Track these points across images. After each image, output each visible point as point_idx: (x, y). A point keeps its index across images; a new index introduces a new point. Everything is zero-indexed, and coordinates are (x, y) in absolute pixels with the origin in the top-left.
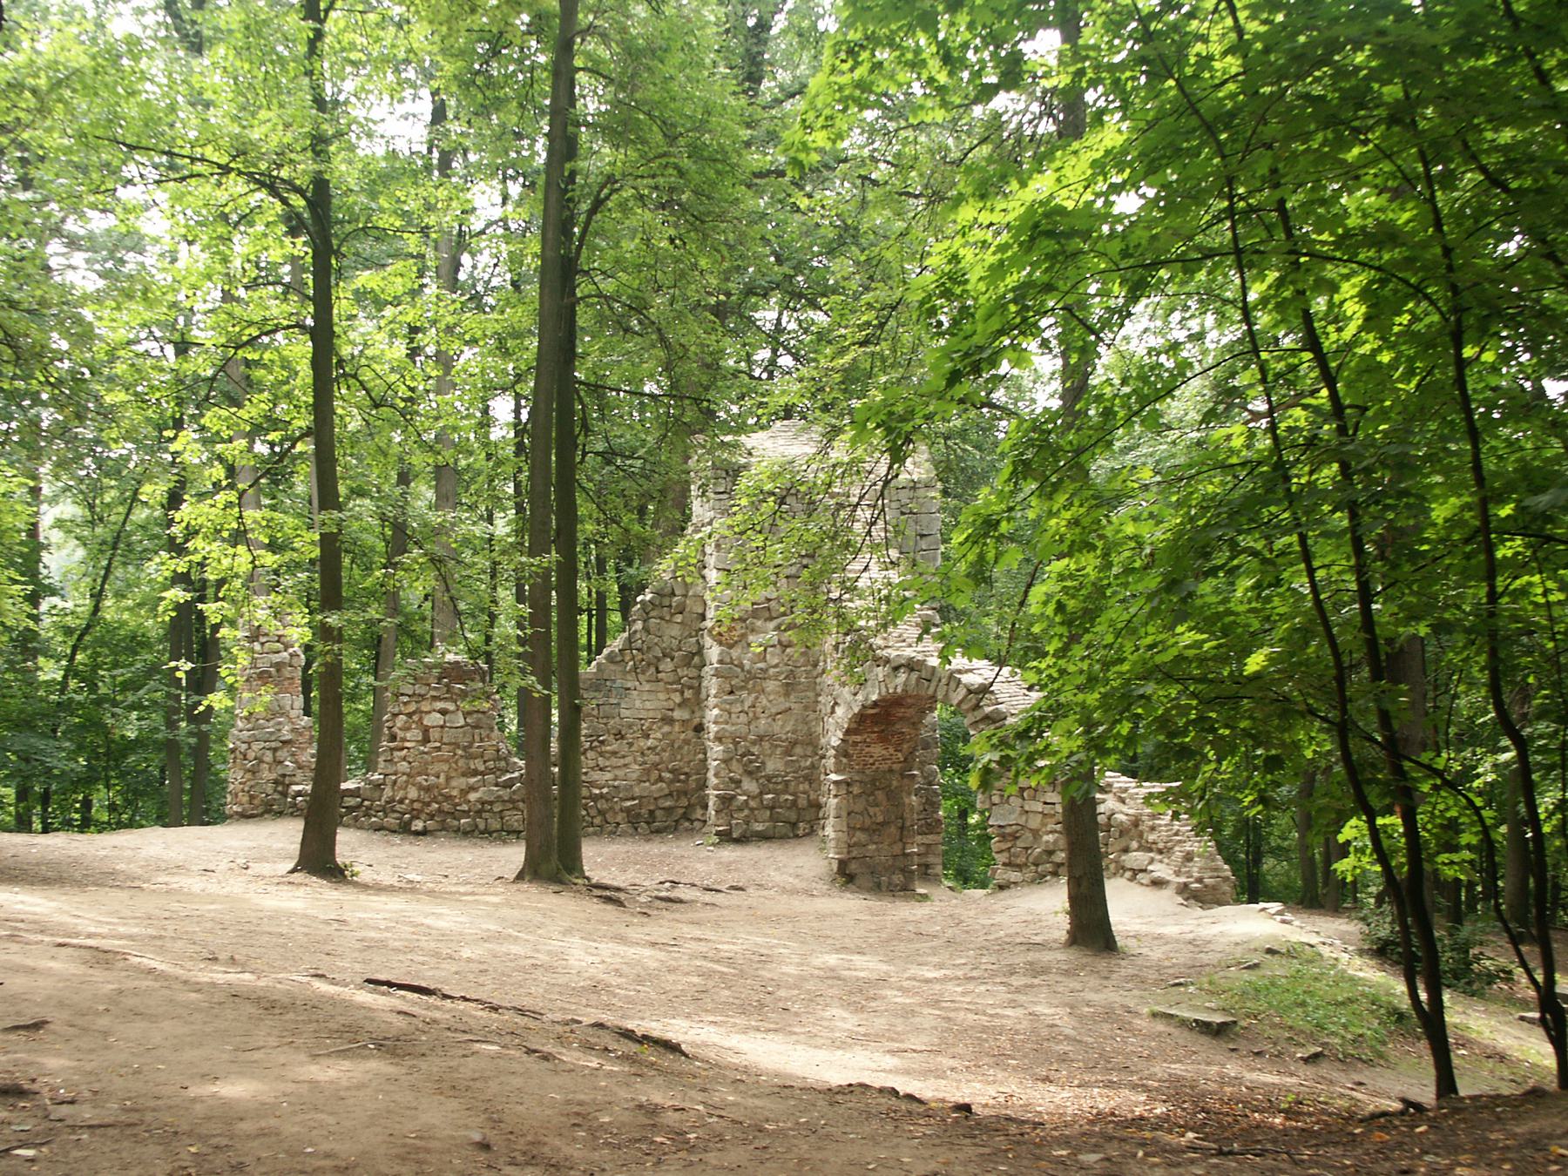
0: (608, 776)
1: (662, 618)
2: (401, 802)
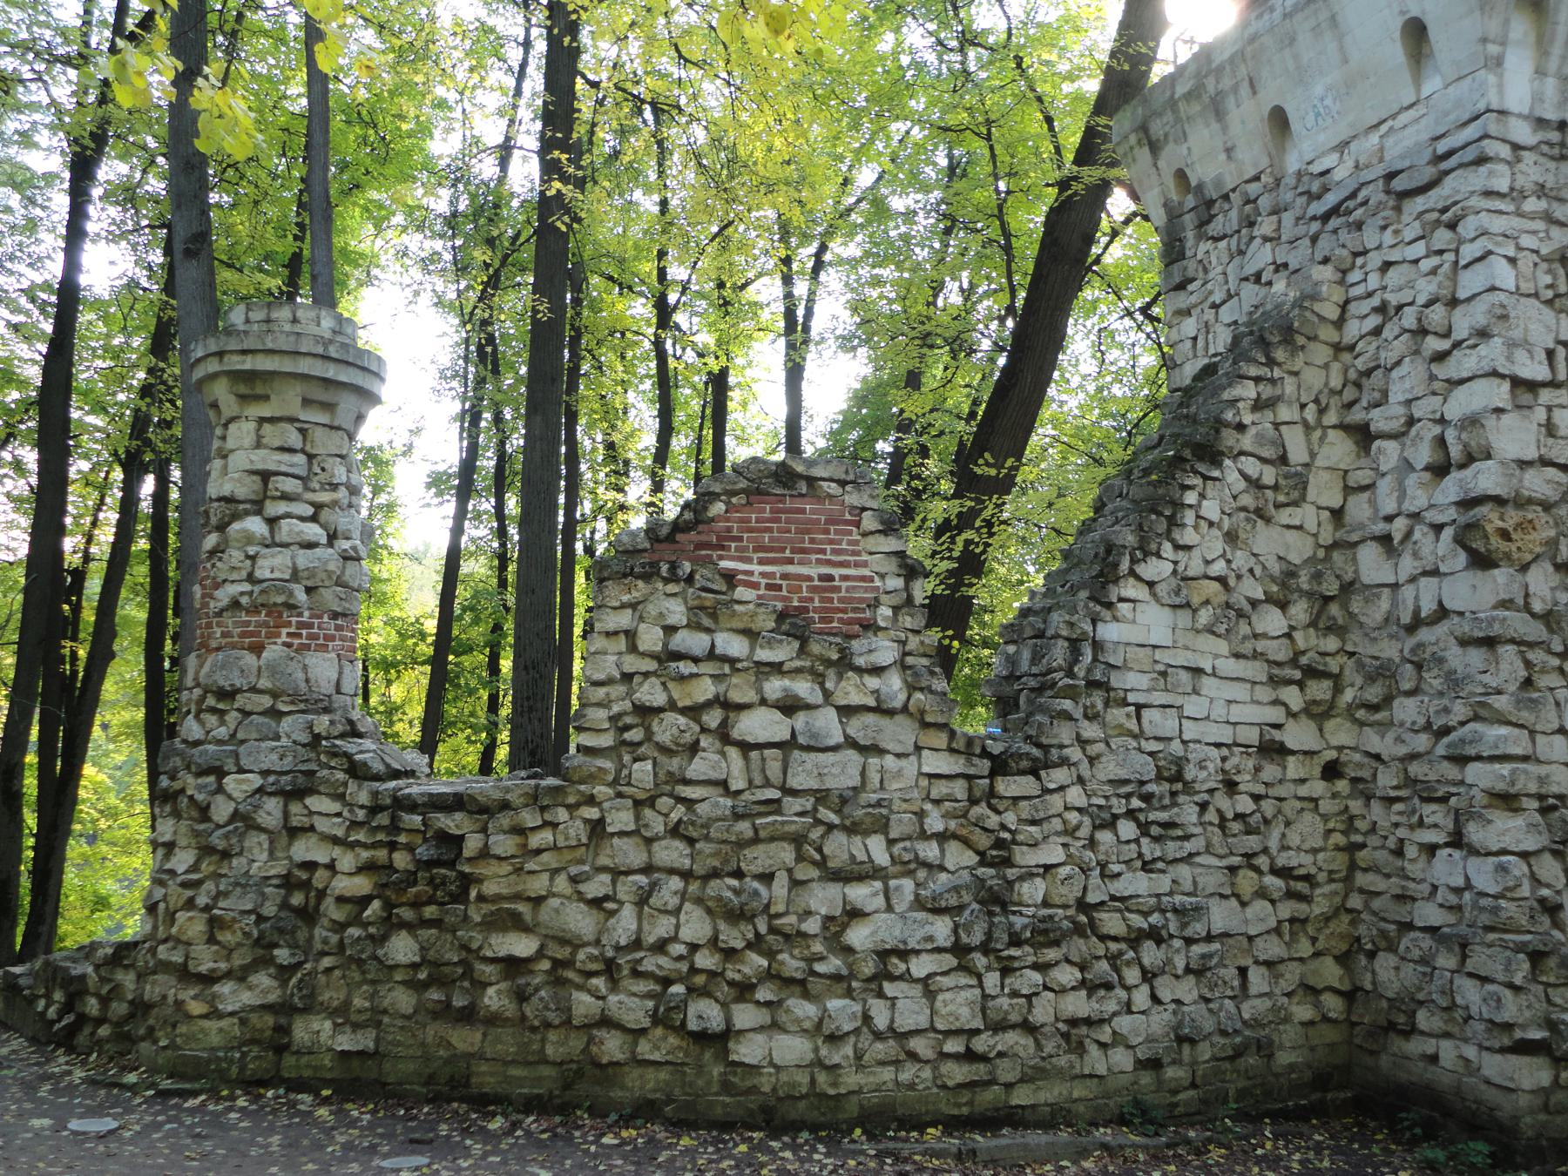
0: (1164, 883)
1: (1259, 513)
2: (661, 947)
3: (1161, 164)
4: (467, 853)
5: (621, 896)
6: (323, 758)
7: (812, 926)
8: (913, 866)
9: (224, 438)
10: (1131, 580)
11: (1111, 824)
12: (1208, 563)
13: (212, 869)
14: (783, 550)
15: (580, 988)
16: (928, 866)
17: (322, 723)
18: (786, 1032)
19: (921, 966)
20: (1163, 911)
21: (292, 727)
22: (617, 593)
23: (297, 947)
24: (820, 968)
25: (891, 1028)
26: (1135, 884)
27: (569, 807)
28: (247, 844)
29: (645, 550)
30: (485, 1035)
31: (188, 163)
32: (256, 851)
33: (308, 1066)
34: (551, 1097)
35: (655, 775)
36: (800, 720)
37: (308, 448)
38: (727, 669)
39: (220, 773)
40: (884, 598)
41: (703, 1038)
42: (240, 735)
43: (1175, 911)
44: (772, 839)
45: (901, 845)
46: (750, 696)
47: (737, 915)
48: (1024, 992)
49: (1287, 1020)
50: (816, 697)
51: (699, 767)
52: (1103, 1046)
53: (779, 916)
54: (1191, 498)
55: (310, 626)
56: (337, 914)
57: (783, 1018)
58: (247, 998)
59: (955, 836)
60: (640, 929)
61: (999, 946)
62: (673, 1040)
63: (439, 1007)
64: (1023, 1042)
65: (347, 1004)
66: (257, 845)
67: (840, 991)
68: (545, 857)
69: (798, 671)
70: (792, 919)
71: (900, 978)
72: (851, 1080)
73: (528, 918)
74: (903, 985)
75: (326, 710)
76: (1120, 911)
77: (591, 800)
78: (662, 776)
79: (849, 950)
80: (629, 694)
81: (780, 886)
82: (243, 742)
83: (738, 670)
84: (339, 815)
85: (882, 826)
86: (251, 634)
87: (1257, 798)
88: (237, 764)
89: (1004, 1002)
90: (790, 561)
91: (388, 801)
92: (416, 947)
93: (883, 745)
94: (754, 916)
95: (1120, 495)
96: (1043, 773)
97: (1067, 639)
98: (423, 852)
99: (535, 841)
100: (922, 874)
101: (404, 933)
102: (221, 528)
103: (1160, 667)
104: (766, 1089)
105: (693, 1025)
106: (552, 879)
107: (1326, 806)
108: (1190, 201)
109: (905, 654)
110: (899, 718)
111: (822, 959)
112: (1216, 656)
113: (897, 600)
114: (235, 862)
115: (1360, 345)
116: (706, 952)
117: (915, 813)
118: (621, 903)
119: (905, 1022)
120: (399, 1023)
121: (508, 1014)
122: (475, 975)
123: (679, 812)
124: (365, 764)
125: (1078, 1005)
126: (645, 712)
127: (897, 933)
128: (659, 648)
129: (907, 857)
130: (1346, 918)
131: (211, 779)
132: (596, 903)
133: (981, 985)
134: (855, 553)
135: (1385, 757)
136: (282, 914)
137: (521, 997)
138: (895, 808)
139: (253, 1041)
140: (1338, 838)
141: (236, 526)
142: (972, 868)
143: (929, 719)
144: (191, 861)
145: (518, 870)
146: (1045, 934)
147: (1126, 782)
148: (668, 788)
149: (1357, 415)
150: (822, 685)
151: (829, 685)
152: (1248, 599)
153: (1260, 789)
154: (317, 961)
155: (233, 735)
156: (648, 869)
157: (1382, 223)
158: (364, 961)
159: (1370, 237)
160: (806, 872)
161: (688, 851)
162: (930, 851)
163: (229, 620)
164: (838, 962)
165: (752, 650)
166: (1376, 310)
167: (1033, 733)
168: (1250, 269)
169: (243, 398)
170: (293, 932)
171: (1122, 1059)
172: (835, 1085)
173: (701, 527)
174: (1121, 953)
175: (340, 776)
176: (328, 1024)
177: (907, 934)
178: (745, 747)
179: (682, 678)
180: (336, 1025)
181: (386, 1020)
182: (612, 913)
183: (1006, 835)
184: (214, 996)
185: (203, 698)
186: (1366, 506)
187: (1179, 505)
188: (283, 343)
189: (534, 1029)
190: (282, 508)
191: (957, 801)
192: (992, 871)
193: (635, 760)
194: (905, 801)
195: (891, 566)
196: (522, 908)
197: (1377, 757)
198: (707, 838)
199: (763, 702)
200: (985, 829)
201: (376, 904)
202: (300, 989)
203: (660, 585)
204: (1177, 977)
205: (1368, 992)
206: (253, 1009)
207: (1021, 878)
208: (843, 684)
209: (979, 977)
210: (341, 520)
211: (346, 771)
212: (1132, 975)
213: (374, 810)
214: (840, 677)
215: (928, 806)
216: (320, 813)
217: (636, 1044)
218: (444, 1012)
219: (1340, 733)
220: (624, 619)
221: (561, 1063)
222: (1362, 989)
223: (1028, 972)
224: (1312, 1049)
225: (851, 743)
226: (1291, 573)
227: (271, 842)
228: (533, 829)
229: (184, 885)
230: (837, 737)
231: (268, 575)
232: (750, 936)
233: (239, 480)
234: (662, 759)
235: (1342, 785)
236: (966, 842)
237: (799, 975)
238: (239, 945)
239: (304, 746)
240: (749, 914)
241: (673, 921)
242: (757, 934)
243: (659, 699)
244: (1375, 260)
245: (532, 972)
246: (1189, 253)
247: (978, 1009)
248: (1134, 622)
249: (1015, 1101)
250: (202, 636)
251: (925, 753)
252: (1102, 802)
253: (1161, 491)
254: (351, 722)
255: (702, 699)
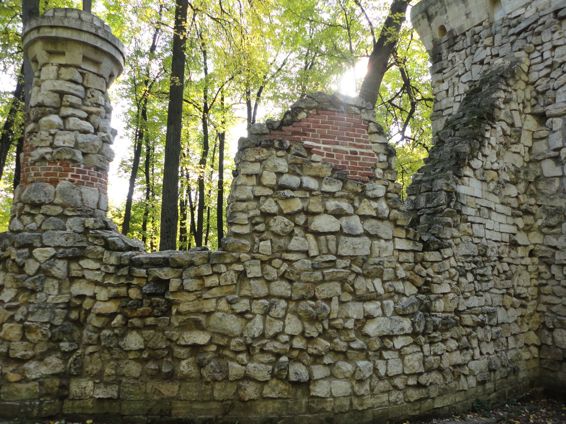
2: (275, 337)
3: (432, 25)
4: (171, 289)
5: (255, 311)
6: (90, 240)
7: (350, 324)
8: (393, 294)
9: (39, 77)
10: (468, 168)
11: (464, 275)
12: (492, 163)
13: (25, 299)
14: (334, 138)
15: (232, 360)
16: (398, 293)
17: (90, 222)
18: (337, 378)
19: (399, 343)
20: (483, 313)
21: (73, 224)
22: (252, 155)
23: (74, 341)
24: (354, 345)
25: (386, 375)
26: (474, 302)
27: (226, 264)
28: (46, 285)
29: (266, 134)
30: (180, 387)
31: (30, 12)
32: (51, 289)
33: (79, 407)
34: (217, 419)
35: (272, 247)
36: (344, 221)
37: (85, 83)
38: (308, 195)
39: (31, 247)
40: (379, 165)
41: (297, 384)
42: (43, 227)
43: (488, 313)
44: (331, 281)
45: (388, 283)
46: (320, 209)
47: (314, 320)
48: (439, 353)
49: (520, 359)
50: (350, 210)
51: (294, 244)
52: (465, 376)
53: (334, 319)
54: (487, 135)
55: (84, 172)
56: (97, 323)
57: (336, 372)
58: (44, 370)
59: (408, 280)
60: (264, 328)
61: (430, 332)
62: (282, 386)
63: (155, 372)
64: (438, 377)
65: (102, 371)
66: (51, 287)
67: (362, 357)
68: (214, 291)
69: (342, 197)
70: (340, 321)
71: (390, 349)
72: (369, 402)
73: (204, 323)
74: (391, 353)
75: (91, 216)
76: (469, 314)
77: (239, 261)
78: (276, 248)
79: (367, 336)
80: (258, 207)
81: (335, 304)
82: (45, 231)
83: (314, 195)
84: (99, 269)
85: (380, 275)
86: (51, 174)
87: (509, 264)
88: (41, 242)
89: (431, 358)
90: (337, 144)
91: (127, 262)
92: (142, 340)
93: (380, 235)
94: (323, 320)
95: (451, 136)
96: (442, 250)
97: (446, 191)
98: (147, 289)
99: (209, 282)
100: (396, 297)
101: (135, 333)
102: (36, 121)
103: (478, 207)
104: (329, 409)
105: (293, 378)
106: (217, 302)
107: (531, 268)
108: (445, 38)
109: (387, 192)
110: (386, 222)
111: (354, 341)
112: (496, 203)
113: (385, 166)
114: (38, 295)
115: (537, 83)
116: (299, 339)
117: (393, 268)
118: (255, 314)
119: (392, 372)
120: (132, 381)
121: (193, 375)
122: (175, 354)
123: (284, 267)
124: (114, 242)
125: (457, 358)
126: (266, 215)
127: (389, 327)
128: (274, 183)
129: (391, 289)
130: (537, 315)
131: (26, 250)
132: (241, 315)
133: (422, 351)
134: (366, 142)
135: (560, 247)
136: (65, 324)
137: (200, 365)
138: (385, 265)
139: (47, 394)
140: (535, 282)
141: (44, 119)
142: (416, 295)
143: (399, 223)
144: (13, 296)
145: (199, 298)
146: (446, 326)
147: (468, 256)
148: (278, 255)
149: (539, 109)
150: (352, 204)
151: (356, 204)
152: (504, 180)
153: (510, 261)
154: (85, 348)
155: (39, 227)
156: (268, 297)
157: (553, 30)
158: (112, 348)
159: (545, 37)
160: (347, 297)
161: (289, 287)
162: (399, 286)
163: (39, 167)
164: (362, 342)
165: (320, 186)
166: (547, 67)
167: (436, 232)
168: (477, 59)
169: (50, 53)
170: (71, 333)
171: (472, 381)
172: (362, 405)
173: (295, 124)
174: (471, 333)
175: (100, 249)
176: (91, 383)
177: (393, 327)
178: (317, 234)
179: (286, 198)
180: (95, 383)
181: (124, 380)
182: (249, 320)
183: (430, 279)
184: (24, 370)
185: (23, 208)
186: (544, 145)
187: (483, 136)
188: (74, 24)
189: (207, 383)
190: (70, 111)
191: (410, 263)
192: (424, 296)
193: (261, 240)
194: (390, 262)
195: (381, 149)
196: (201, 318)
197: (555, 248)
198: (299, 280)
199: (326, 212)
200: (421, 276)
201: (119, 317)
202: (75, 364)
203: (274, 152)
204: (488, 342)
205: (549, 346)
206: (47, 376)
207: (435, 300)
208: (362, 204)
209: (421, 347)
210: (102, 124)
211: (103, 246)
212: (475, 343)
213: (119, 267)
214: (360, 201)
215: (398, 265)
216: (88, 269)
217: (262, 389)
218: (157, 375)
219: (536, 238)
220: (256, 168)
221: (223, 401)
222: (546, 344)
223: (439, 343)
224: (528, 371)
225: (367, 234)
226: (518, 171)
227: (60, 285)
228: (207, 276)
229: (8, 309)
230: (361, 231)
231: (61, 144)
232: (321, 330)
233: (47, 95)
234: (275, 239)
235: (536, 260)
236: (413, 282)
237: (344, 350)
238: (39, 341)
239: (80, 233)
240: (320, 319)
241: (282, 323)
242: (324, 329)
243: (274, 209)
244: (548, 46)
245: (206, 352)
246: (443, 58)
247: (421, 363)
248: (469, 186)
249: (436, 406)
250: (24, 176)
251: (396, 239)
252: (461, 264)
253: (476, 131)
254: (105, 222)
255: (296, 210)
